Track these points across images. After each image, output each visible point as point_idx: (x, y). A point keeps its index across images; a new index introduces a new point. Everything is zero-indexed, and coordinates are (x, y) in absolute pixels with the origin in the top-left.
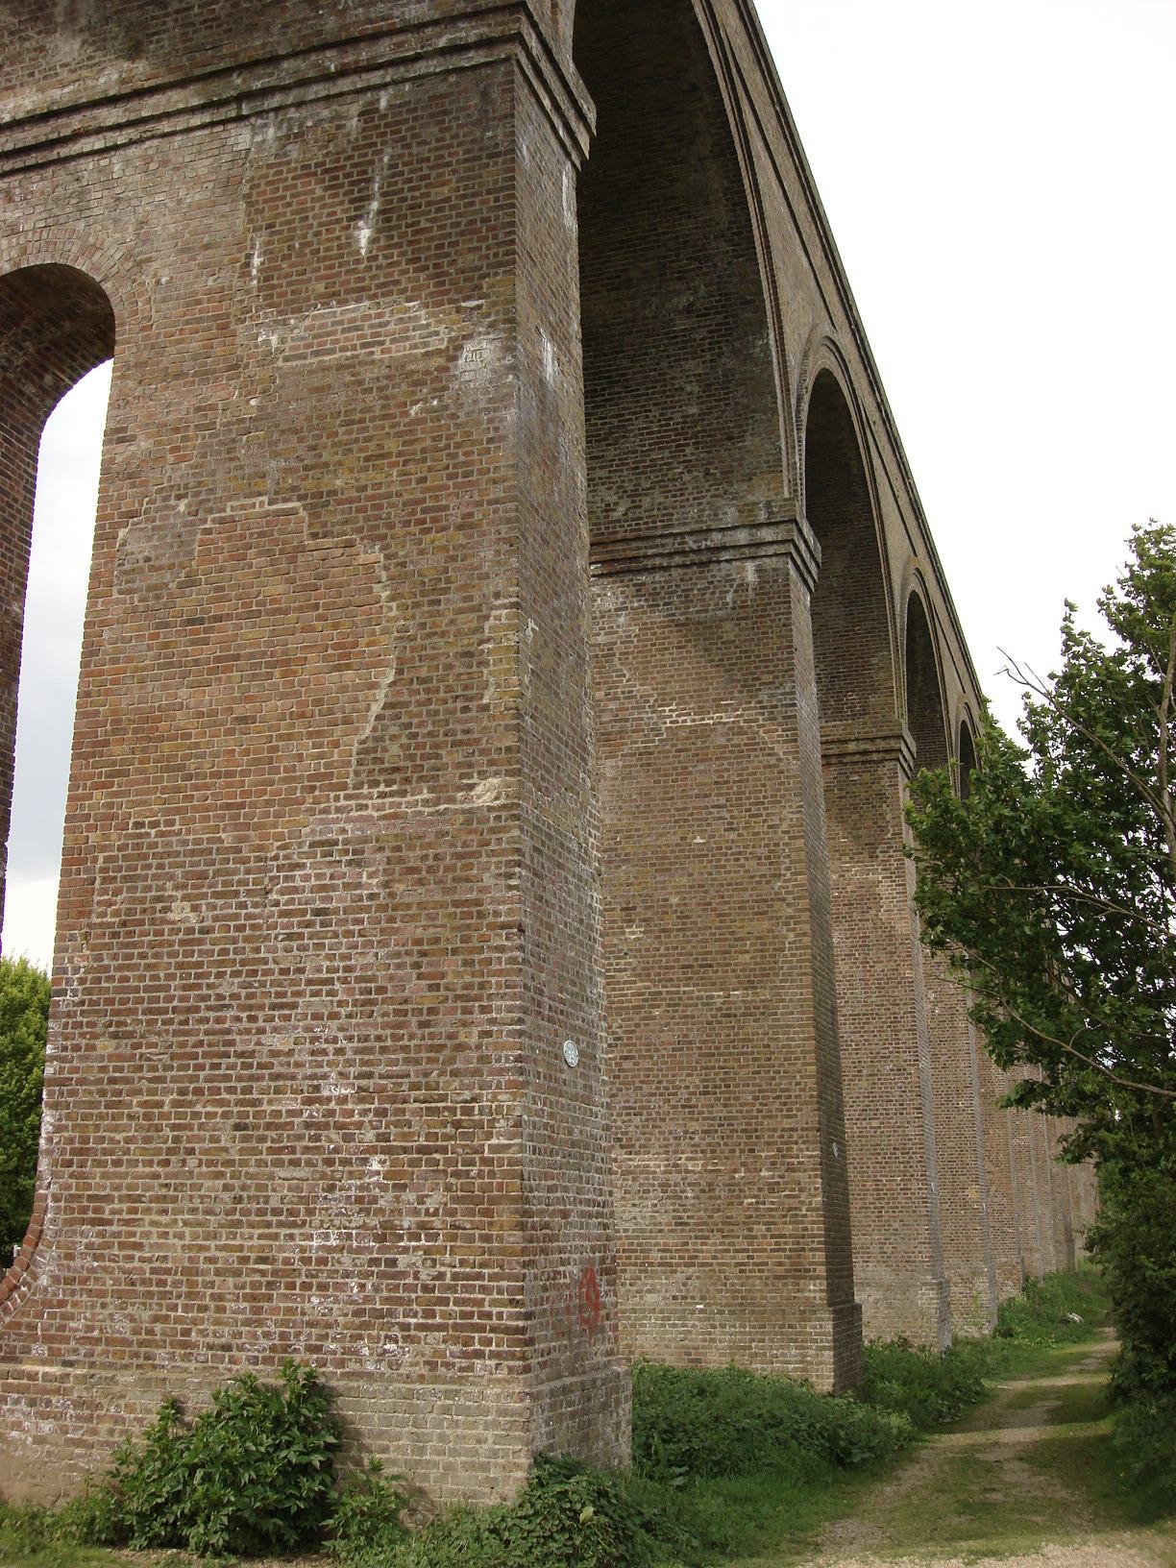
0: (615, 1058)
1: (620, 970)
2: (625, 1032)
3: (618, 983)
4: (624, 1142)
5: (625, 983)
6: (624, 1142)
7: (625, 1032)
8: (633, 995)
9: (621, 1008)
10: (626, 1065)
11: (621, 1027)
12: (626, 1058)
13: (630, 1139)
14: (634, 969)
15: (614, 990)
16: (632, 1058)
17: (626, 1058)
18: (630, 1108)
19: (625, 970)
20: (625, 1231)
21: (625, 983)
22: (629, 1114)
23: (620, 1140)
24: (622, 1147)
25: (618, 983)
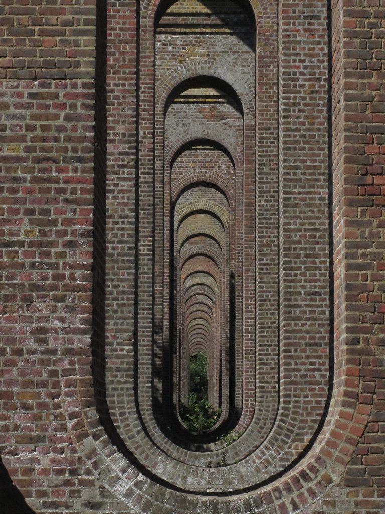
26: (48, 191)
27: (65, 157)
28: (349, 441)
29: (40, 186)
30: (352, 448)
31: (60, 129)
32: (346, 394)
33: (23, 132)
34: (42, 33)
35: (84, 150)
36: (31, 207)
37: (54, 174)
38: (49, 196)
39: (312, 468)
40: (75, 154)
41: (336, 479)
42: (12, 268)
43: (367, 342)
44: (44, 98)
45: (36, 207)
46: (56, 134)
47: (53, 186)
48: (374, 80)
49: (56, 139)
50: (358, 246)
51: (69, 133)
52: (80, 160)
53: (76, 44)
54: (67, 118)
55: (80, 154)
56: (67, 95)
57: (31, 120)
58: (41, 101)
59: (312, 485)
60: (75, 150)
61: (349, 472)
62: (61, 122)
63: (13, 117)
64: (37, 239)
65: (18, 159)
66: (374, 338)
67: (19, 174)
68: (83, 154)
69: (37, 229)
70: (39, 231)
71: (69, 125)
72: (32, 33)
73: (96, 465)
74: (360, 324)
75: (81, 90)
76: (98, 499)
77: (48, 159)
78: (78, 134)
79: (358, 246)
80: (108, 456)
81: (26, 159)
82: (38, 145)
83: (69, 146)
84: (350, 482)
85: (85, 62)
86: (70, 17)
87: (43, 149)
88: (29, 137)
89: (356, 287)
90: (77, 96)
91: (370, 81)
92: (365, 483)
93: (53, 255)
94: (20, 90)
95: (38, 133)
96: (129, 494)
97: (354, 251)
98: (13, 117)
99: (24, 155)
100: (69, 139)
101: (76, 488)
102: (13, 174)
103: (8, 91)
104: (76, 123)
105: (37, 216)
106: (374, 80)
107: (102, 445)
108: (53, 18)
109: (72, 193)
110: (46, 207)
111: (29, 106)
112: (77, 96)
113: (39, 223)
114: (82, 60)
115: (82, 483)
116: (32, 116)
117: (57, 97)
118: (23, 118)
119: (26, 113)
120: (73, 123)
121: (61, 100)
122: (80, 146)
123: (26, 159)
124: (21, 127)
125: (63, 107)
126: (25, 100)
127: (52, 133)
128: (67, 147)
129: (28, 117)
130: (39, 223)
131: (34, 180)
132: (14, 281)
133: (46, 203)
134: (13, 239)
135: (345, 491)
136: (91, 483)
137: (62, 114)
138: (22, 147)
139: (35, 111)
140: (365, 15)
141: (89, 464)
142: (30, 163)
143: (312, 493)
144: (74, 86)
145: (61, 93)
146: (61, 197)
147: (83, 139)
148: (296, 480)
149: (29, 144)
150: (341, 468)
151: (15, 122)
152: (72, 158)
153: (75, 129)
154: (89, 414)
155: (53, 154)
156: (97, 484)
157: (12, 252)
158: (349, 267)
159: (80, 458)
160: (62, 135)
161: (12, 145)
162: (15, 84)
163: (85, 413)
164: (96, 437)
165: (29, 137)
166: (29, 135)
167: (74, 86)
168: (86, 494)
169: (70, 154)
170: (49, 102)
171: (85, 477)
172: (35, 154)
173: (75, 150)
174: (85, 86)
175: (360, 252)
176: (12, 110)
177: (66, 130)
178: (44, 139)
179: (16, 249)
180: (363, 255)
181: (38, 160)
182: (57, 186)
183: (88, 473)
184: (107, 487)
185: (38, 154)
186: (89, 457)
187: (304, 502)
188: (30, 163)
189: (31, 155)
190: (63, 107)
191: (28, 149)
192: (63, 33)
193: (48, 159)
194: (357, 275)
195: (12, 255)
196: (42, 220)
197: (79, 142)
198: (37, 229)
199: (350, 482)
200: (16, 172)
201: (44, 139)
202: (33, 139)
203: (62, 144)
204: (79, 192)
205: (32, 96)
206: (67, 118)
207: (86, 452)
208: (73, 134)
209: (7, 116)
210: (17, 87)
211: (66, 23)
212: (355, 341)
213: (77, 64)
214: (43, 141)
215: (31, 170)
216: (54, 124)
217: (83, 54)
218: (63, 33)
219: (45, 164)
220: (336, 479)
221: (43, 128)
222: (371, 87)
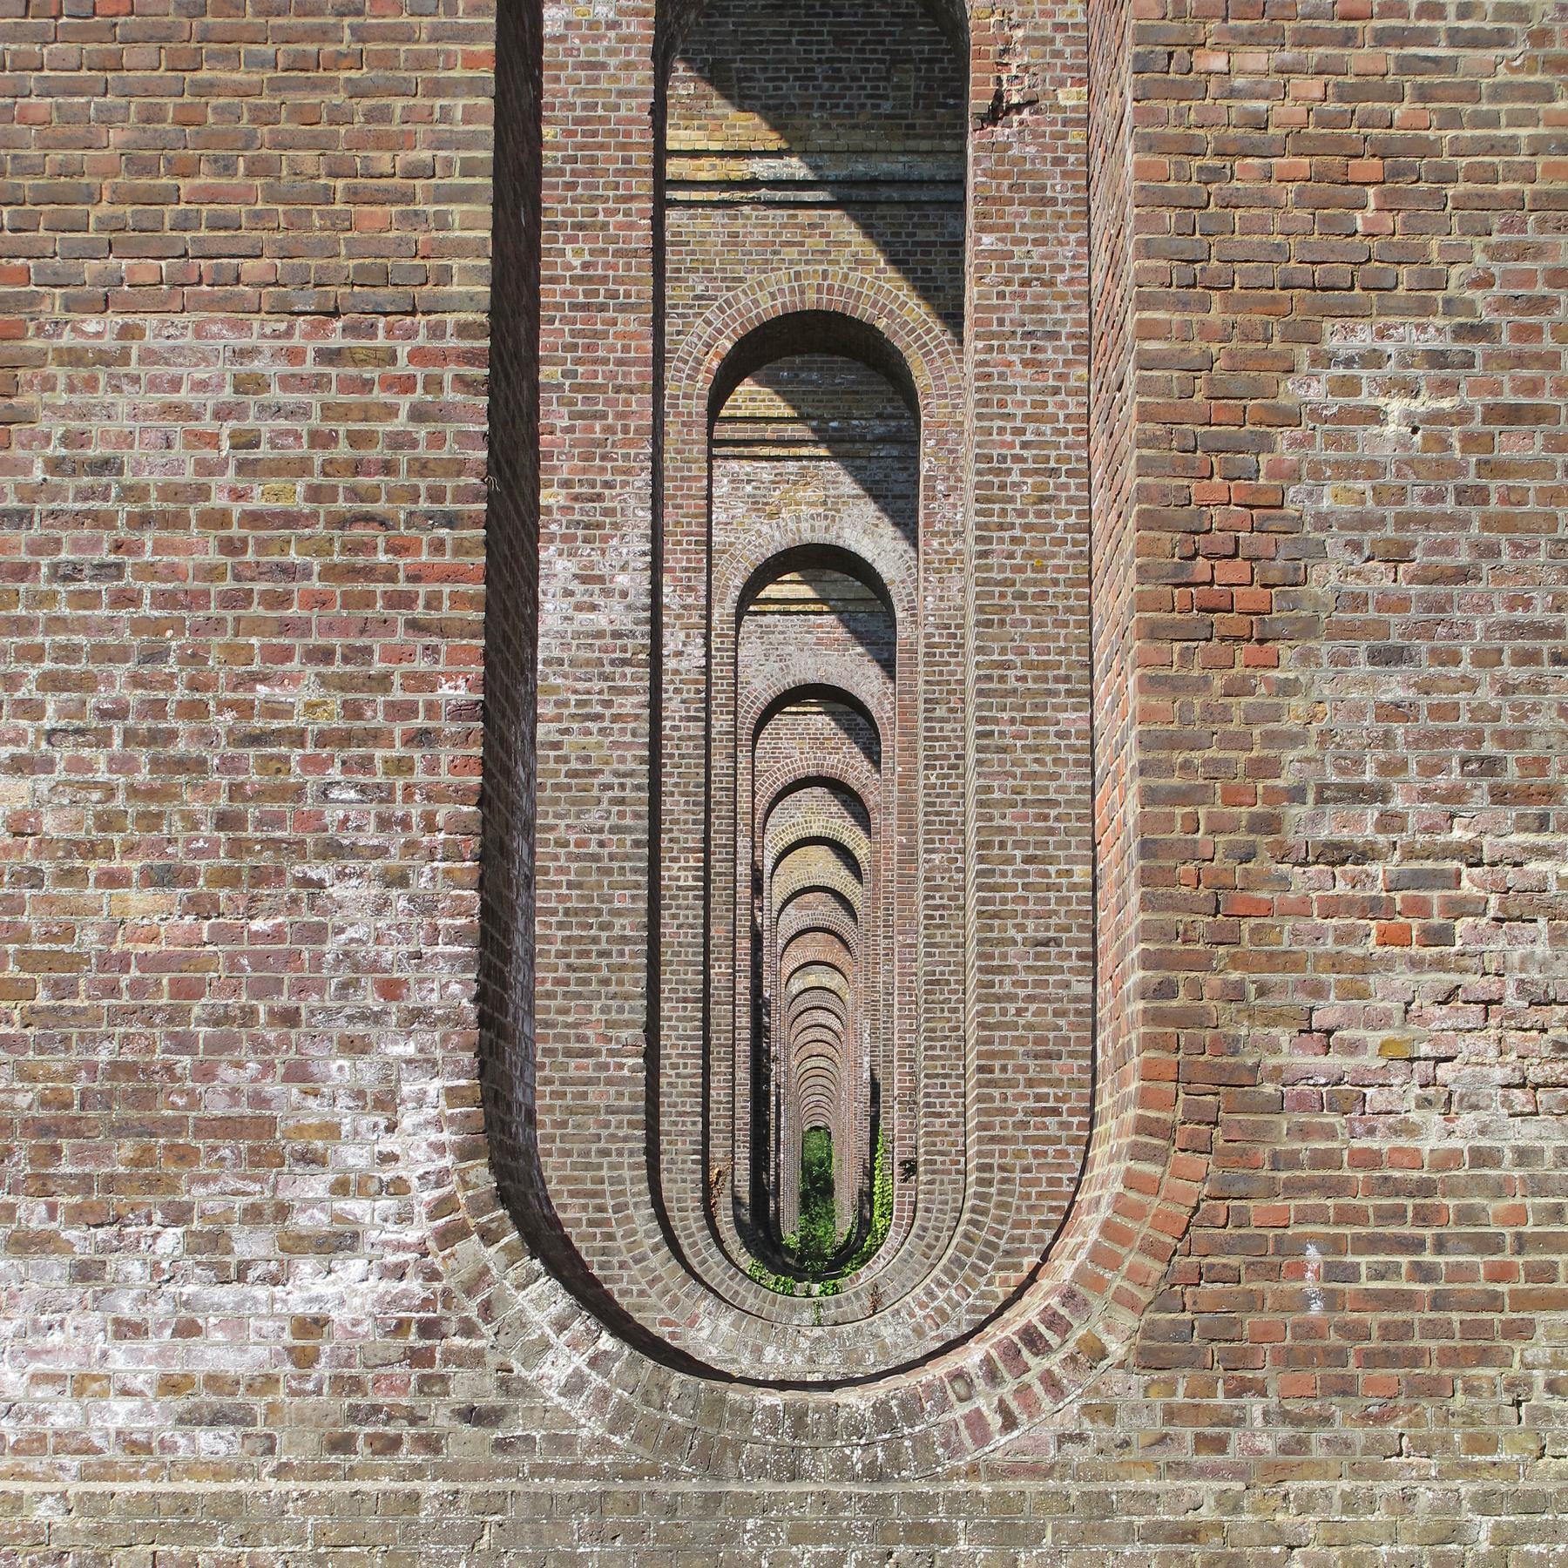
0: (1463, 416)
1: (1475, 40)
2: (1503, 305)
3: (1473, 93)
4: (1512, 775)
5: (1498, 94)
6: (1512, 775)
7: (1503, 305)
8: (1538, 147)
9: (1486, 204)
10: (1514, 445)
11: (1485, 282)
12: (1512, 415)
13: (1541, 764)
14: (1541, 37)
15: (1452, 120)
16: (1540, 415)
17: (1512, 415)
18: (1541, 631)
19: (1501, 39)
20: (1524, 1156)
21: (1498, 94)
22: (1527, 658)
23: (1490, 766)
24: (1500, 796)
25: (1473, 93)
26: (367, 600)
27: (411, 514)
28: (1149, 1249)
29: (347, 587)
30: (1158, 1268)
31: (400, 441)
32: (1143, 1126)
33: (303, 450)
34: (354, 196)
35: (462, 495)
36: (321, 641)
37: (382, 558)
38: (369, 613)
39: (1053, 1320)
40: (436, 507)
41: (1117, 1348)
42: (274, 799)
43: (1197, 992)
44: (356, 363)
45: (337, 642)
46: (389, 454)
47: (380, 588)
48: (1216, 315)
49: (388, 468)
50: (1173, 743)
51: (421, 451)
52: (451, 521)
53: (443, 223)
54: (418, 414)
55: (448, 506)
56: (416, 356)
57: (325, 418)
58: (351, 371)
59: (1053, 1362)
60: (436, 495)
61: (1149, 1332)
62: (400, 423)
63: (278, 411)
64: (339, 724)
65: (290, 519)
66: (1214, 980)
67: (293, 557)
68: (458, 507)
69: (336, 700)
70: (345, 704)
71: (422, 432)
72: (328, 196)
73: (487, 1309)
74: (1177, 946)
75: (452, 342)
76: (495, 1400)
77: (367, 519)
78: (444, 454)
79: (1173, 743)
80: (521, 1287)
81: (310, 519)
82: (342, 482)
83: (422, 484)
84: (1150, 1359)
85: (463, 269)
86: (426, 155)
87: (354, 494)
88: (317, 462)
89: (1168, 848)
90: (443, 357)
91: (1202, 316)
92: (1191, 1360)
93: (379, 764)
94: (296, 341)
95: (343, 451)
96: (574, 1386)
97: (1163, 755)
98: (278, 411)
99: (307, 508)
100: (422, 468)
101: (438, 1369)
102: (276, 558)
103: (266, 344)
104: (440, 426)
105: (338, 667)
106: (1216, 315)
107: (504, 1259)
108: (383, 160)
109: (428, 606)
110: (360, 642)
111: (320, 383)
112: (443, 357)
113: (344, 684)
114: (455, 263)
115: (451, 1356)
116: (326, 408)
117: (392, 358)
118: (301, 412)
119: (313, 399)
120: (433, 426)
121: (403, 367)
122: (450, 484)
123: (310, 519)
124: (298, 437)
125: (407, 384)
126: (309, 367)
127: (378, 453)
128: (416, 487)
129: (316, 411)
130: (344, 684)
131: (329, 573)
132: (278, 834)
133: (362, 632)
134: (276, 724)
135: (1138, 1380)
136: (477, 1357)
137: (405, 402)
138: (300, 488)
139: (333, 396)
140: (1192, 150)
141: (472, 1311)
142: (320, 529)
143: (1052, 1384)
144: (437, 331)
145: (403, 349)
146: (401, 616)
147: (460, 467)
148: (1011, 1353)
149: (318, 479)
150: (1128, 1320)
151: (283, 424)
152: (429, 515)
153: (437, 440)
154: (471, 1177)
155: (381, 507)
156: (492, 1360)
157: (271, 757)
158: (1150, 796)
159: (447, 1293)
160: (403, 457)
161: (275, 483)
162: (283, 327)
163: (463, 1174)
164: (488, 1237)
165: (317, 462)
166: (319, 456)
167: (437, 331)
168: (465, 1386)
169: (424, 505)
170: (370, 372)
171: (458, 1341)
172: (333, 507)
173: (436, 495)
174: (463, 330)
175: (1179, 757)
176: (276, 394)
177: (414, 444)
178: (357, 468)
179: (284, 750)
180: (1186, 765)
181: (342, 522)
182: (389, 587)
183: (468, 1329)
184: (517, 1368)
185: (342, 505)
186: (470, 1292)
187: (1031, 1406)
188: (320, 529)
189: (322, 509)
190: (407, 384)
191: (314, 494)
192: (409, 198)
193: (367, 519)
194: (1171, 818)
195: (275, 765)
196: (352, 676)
197: (446, 474)
198: (336, 700)
199: (1150, 1359)
200: (283, 552)
201: (357, 468)
202: (329, 468)
203: (403, 479)
204: (446, 603)
205: (329, 356)
206: (418, 414)
207: (464, 1275)
208: (433, 454)
209: (263, 408)
210: (288, 333)
211: (415, 172)
212: (1165, 990)
213: (445, 276)
214: (356, 473)
215: (323, 549)
216: (382, 428)
217: (460, 249)
218: (409, 198)
219: (359, 532)
220: (1117, 1348)
221: (355, 439)
222: (1206, 333)
